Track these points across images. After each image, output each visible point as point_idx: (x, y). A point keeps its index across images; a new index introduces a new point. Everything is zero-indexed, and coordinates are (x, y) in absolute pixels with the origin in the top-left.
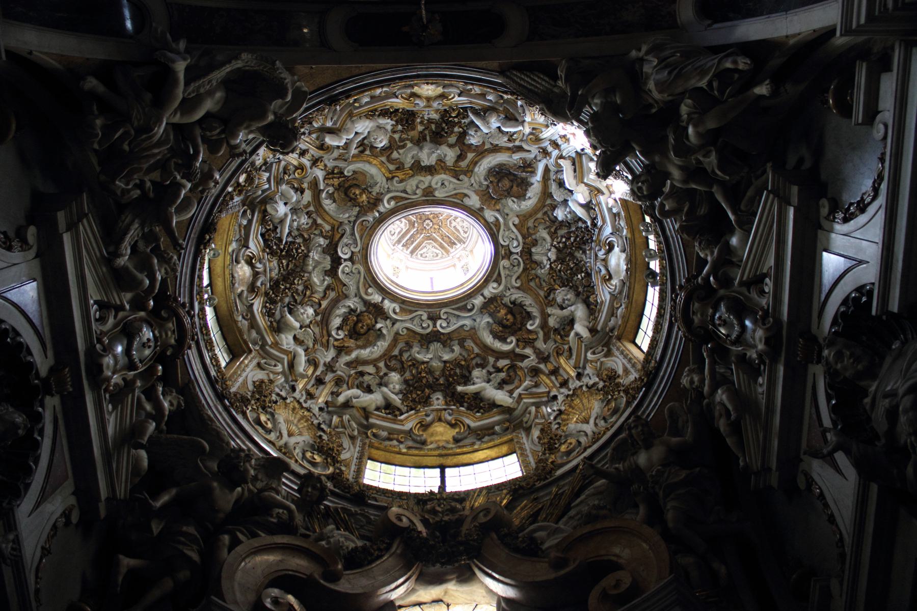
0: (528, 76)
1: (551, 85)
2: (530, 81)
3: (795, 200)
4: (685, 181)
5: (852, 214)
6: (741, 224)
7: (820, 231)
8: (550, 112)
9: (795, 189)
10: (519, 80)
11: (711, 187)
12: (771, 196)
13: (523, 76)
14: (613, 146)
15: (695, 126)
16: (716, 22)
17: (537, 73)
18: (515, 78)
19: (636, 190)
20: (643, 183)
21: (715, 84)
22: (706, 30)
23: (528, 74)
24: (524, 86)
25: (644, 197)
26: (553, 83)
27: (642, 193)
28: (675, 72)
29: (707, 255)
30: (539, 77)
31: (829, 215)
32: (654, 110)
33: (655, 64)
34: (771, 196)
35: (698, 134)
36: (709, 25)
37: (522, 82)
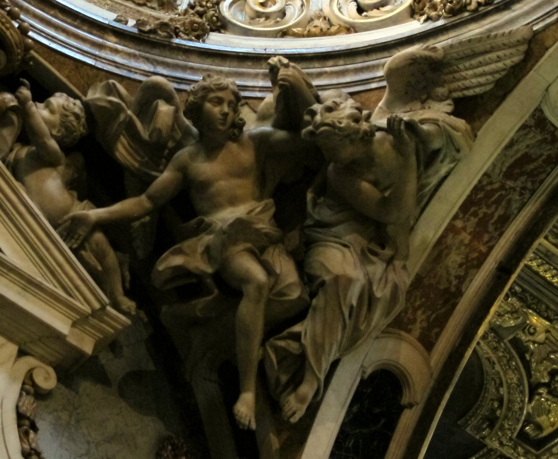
0: (491, 73)
1: (455, 90)
2: (486, 68)
3: (72, 340)
4: (183, 170)
5: (27, 434)
6: (77, 221)
7: (13, 349)
8: (421, 57)
9: (88, 348)
10: (500, 53)
11: (150, 198)
12: (97, 306)
13: (500, 65)
14: (312, 133)
15: (260, 288)
16: (362, 381)
17: (488, 88)
18: (507, 52)
19: (220, 94)
20: (225, 115)
21: (293, 346)
22: (362, 366)
23: (498, 76)
24: (486, 52)
25: (204, 98)
26: (455, 95)
27: (210, 101)
28: (346, 313)
29: (52, 112)
30: (480, 85)
31: (34, 385)
32: (309, 196)
33: (375, 288)
34: (97, 306)
35: (246, 279)
36: (364, 372)
37: (493, 55)
